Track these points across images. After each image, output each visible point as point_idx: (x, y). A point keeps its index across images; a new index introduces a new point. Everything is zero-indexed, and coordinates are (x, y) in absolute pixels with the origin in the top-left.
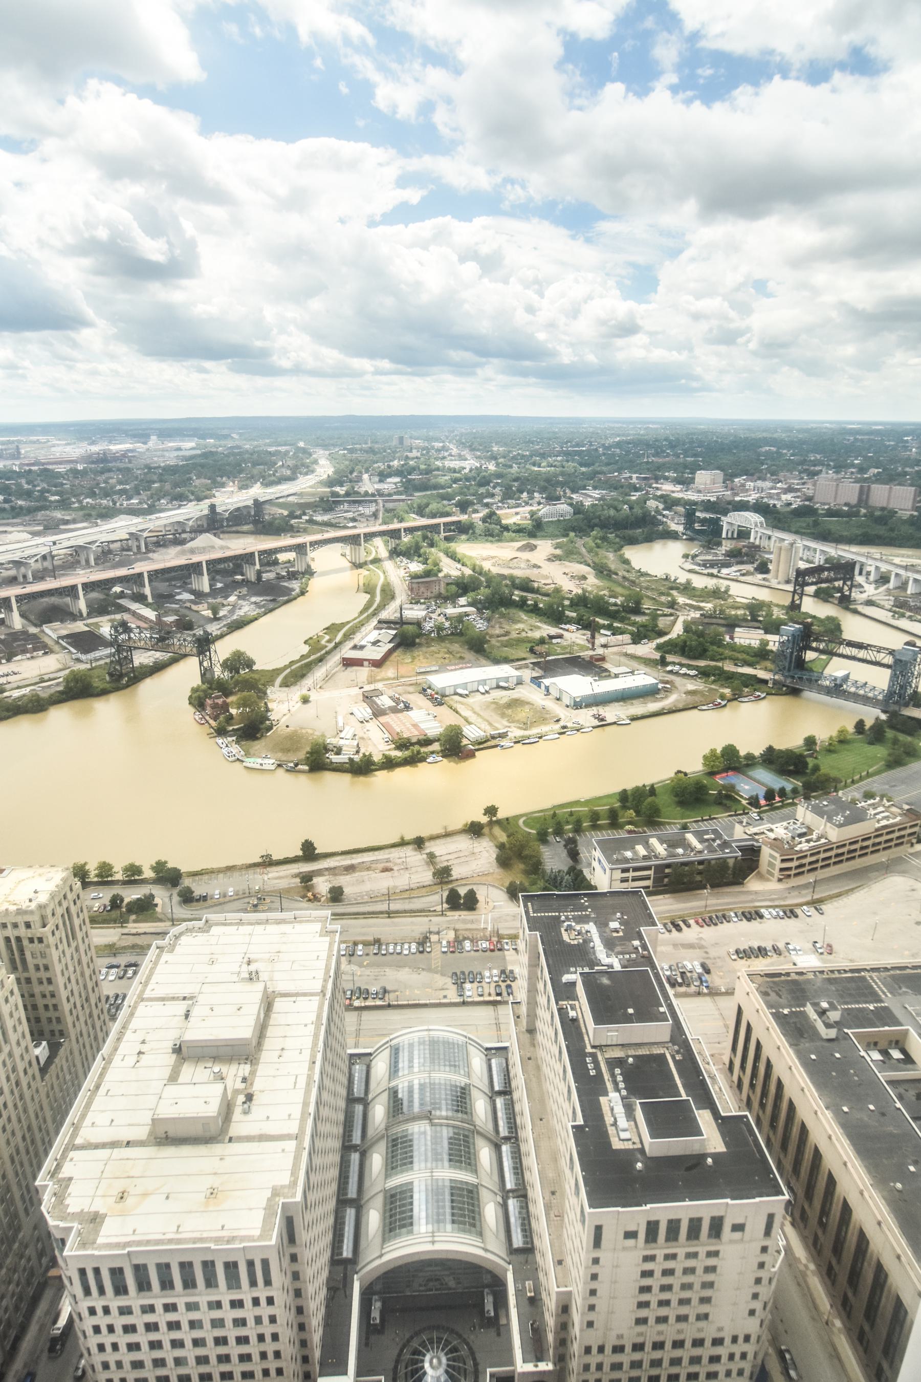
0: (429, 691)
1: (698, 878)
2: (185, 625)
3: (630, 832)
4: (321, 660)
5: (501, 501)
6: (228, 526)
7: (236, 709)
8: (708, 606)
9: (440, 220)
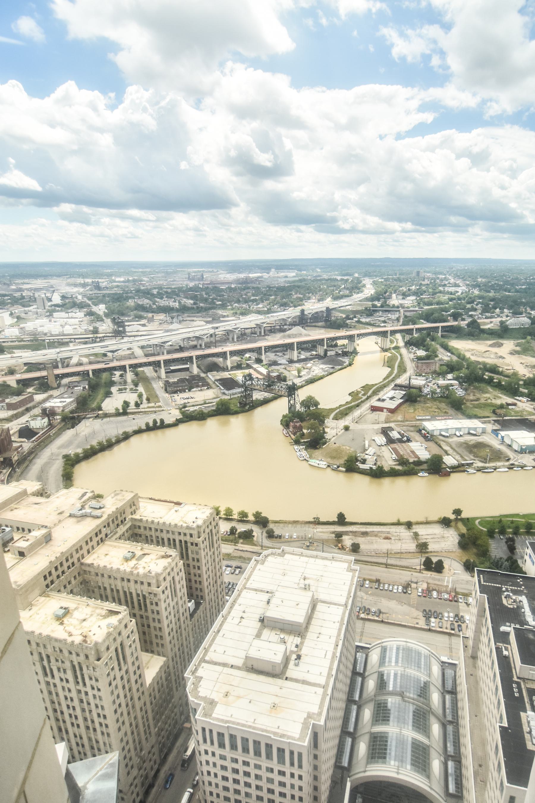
4: (358, 406)
6: (310, 322)
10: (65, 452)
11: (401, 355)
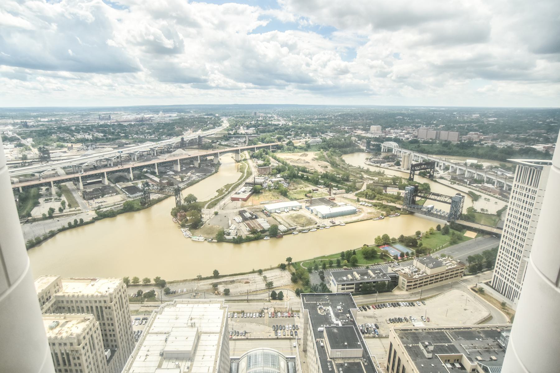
1: (373, 289)
2: (170, 184)
3: (345, 269)
4: (223, 198)
5: (294, 137)
7: (190, 216)
8: (376, 179)
9: (273, 32)
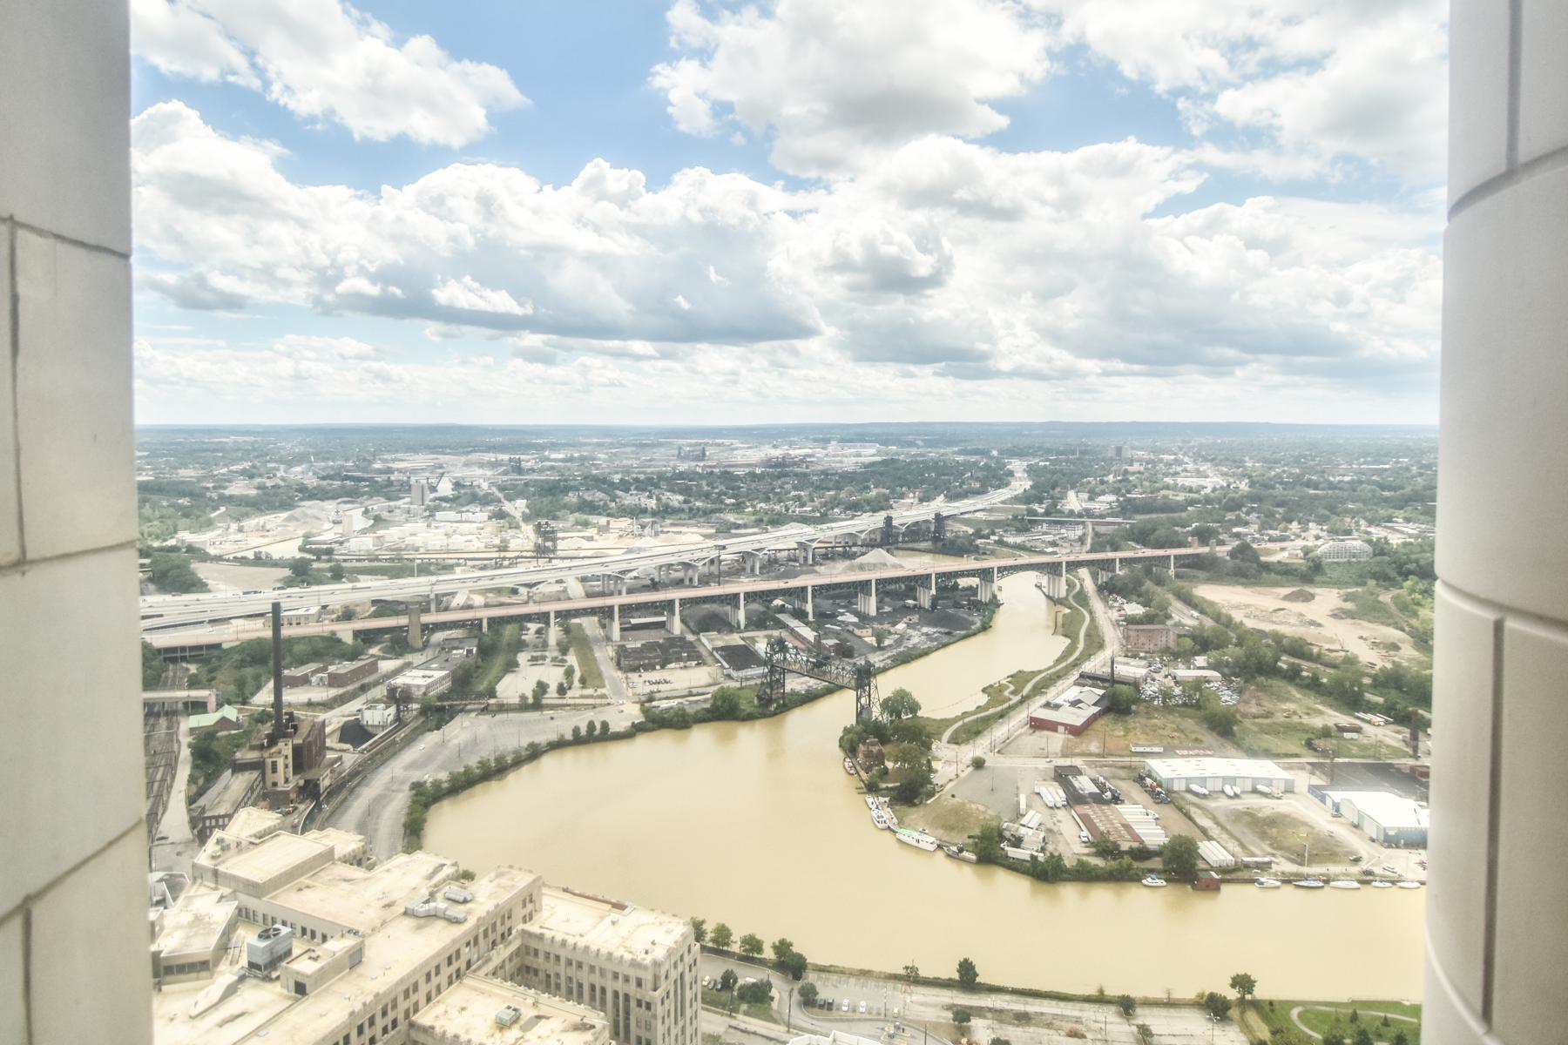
0: (1149, 781)
2: (845, 651)
4: (1002, 715)
7: (893, 759)
10: (416, 776)
11: (1091, 613)
